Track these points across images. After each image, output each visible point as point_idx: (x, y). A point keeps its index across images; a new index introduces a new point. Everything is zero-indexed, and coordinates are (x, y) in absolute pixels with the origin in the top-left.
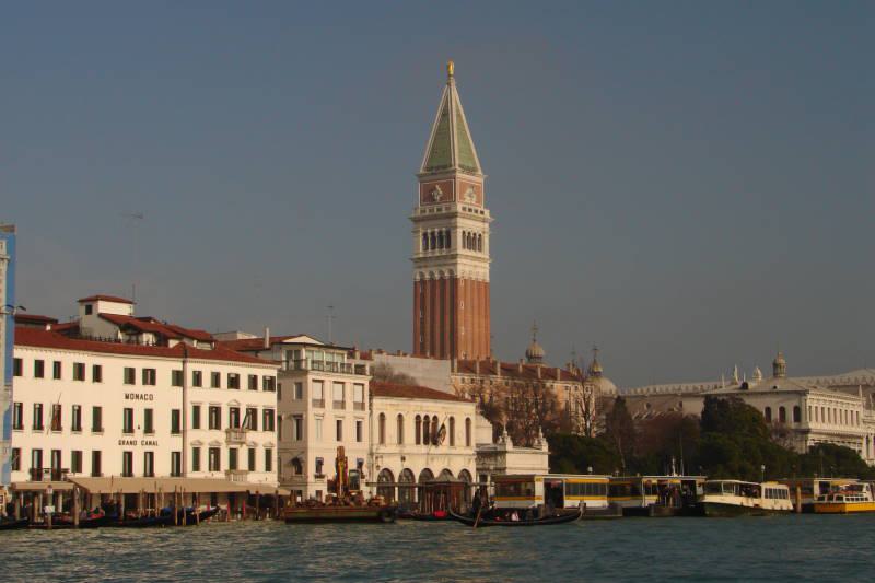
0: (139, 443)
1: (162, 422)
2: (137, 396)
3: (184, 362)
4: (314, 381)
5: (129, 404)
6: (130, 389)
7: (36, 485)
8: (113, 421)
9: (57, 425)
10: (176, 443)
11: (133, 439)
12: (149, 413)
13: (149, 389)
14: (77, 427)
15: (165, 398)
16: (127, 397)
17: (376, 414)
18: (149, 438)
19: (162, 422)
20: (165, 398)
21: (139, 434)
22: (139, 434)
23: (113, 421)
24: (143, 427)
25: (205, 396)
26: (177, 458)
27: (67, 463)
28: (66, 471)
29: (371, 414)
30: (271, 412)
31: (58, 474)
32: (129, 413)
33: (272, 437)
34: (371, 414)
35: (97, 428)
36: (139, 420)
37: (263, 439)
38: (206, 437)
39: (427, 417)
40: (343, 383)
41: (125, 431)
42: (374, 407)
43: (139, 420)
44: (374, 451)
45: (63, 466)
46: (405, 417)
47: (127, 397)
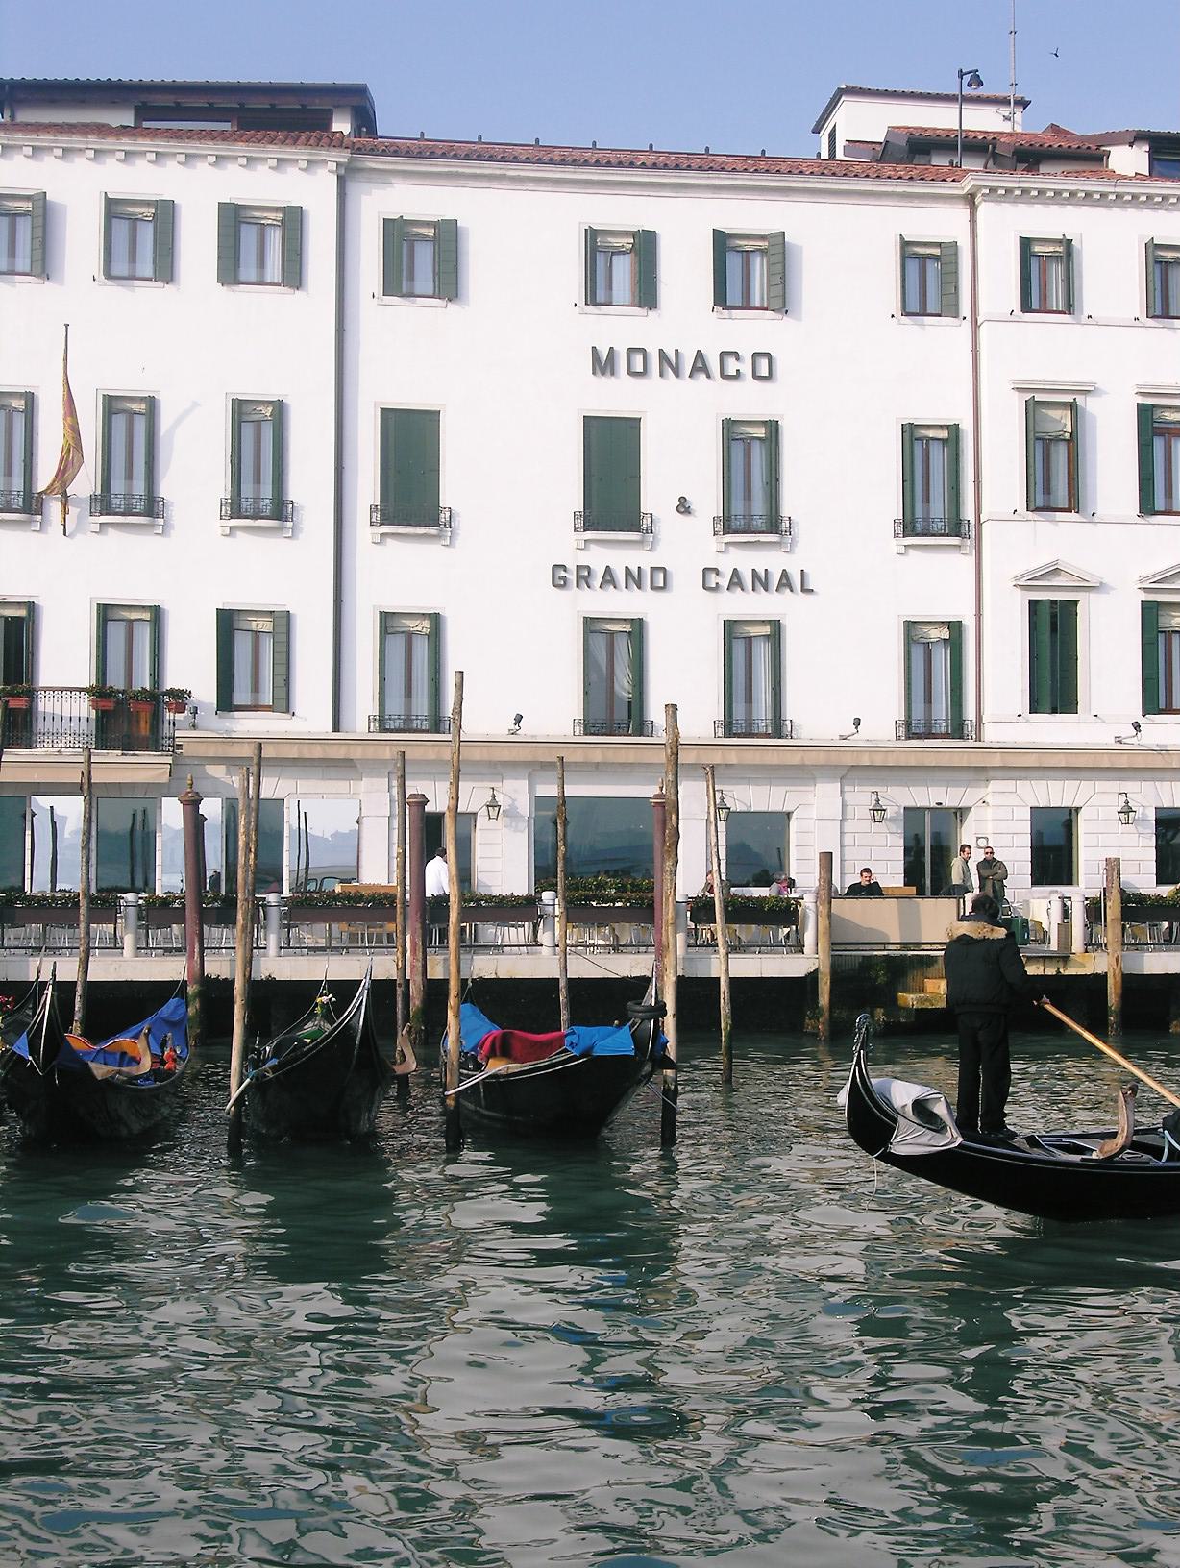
2: (670, 364)
5: (615, 398)
6: (621, 328)
8: (513, 479)
9: (132, 497)
10: (937, 582)
11: (639, 559)
13: (748, 331)
16: (603, 365)
19: (838, 486)
20: (850, 374)
23: (513, 479)
24: (709, 503)
26: (935, 655)
27: (190, 666)
28: (180, 697)
36: (679, 467)
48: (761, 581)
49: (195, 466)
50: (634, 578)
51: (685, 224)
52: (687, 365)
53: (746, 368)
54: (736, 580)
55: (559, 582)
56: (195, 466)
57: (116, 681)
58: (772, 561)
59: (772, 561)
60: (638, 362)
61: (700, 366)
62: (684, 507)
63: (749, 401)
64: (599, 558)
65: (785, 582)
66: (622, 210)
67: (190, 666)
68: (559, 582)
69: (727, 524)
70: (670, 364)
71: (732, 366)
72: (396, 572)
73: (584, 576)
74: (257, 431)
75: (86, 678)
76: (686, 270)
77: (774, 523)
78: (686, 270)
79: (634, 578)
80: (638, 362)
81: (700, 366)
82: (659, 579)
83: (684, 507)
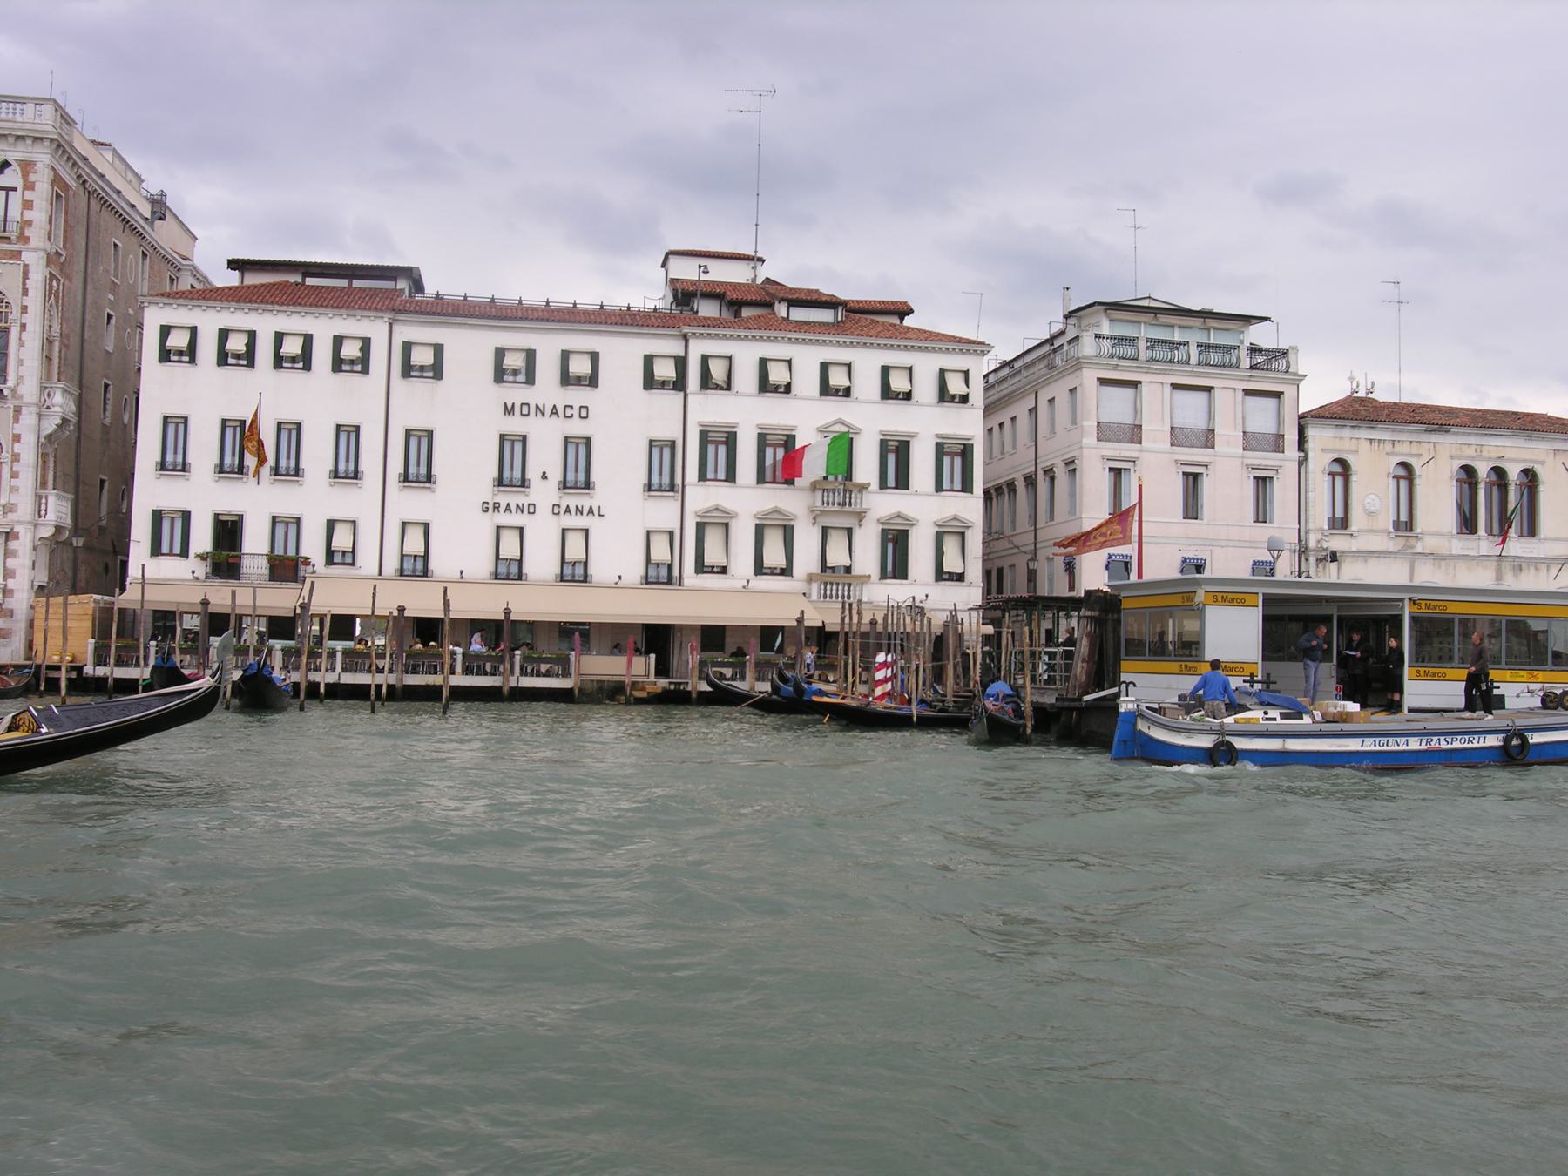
0: (544, 509)
1: (620, 469)
2: (540, 410)
3: (685, 338)
4: (1103, 382)
5: (515, 425)
6: (517, 394)
7: (221, 596)
10: (664, 513)
11: (523, 500)
12: (579, 450)
13: (577, 396)
14: (346, 473)
15: (626, 419)
16: (509, 411)
17: (1319, 461)
18: (572, 501)
19: (620, 469)
21: (544, 493)
22: (544, 493)
23: (466, 463)
24: (556, 475)
25: (746, 413)
28: (306, 561)
29: (1303, 462)
30: (966, 452)
31: (285, 568)
32: (512, 447)
33: (971, 508)
34: (1303, 462)
35: (346, 473)
36: (545, 456)
37: (924, 506)
38: (747, 500)
39: (1499, 472)
40: (1209, 389)
41: (500, 482)
42: (1311, 445)
43: (545, 456)
44: (1312, 544)
45: (303, 553)
46: (1417, 470)
47: (509, 411)
48: (579, 511)
49: (317, 452)
50: (520, 508)
51: (548, 346)
52: (548, 412)
53: (576, 412)
54: (568, 510)
55: (485, 510)
56: (317, 452)
57: (279, 551)
58: (585, 502)
59: (585, 502)
60: (525, 410)
61: (554, 412)
62: (544, 477)
63: (577, 428)
64: (503, 500)
65: (591, 511)
66: (516, 339)
67: (312, 547)
68: (485, 510)
69: (564, 485)
70: (540, 410)
71: (569, 413)
72: (409, 504)
73: (496, 507)
74: (348, 435)
75: (266, 549)
76: (547, 369)
77: (588, 485)
78: (547, 369)
79: (520, 508)
80: (525, 410)
81: (554, 412)
82: (532, 509)
83: (544, 477)
